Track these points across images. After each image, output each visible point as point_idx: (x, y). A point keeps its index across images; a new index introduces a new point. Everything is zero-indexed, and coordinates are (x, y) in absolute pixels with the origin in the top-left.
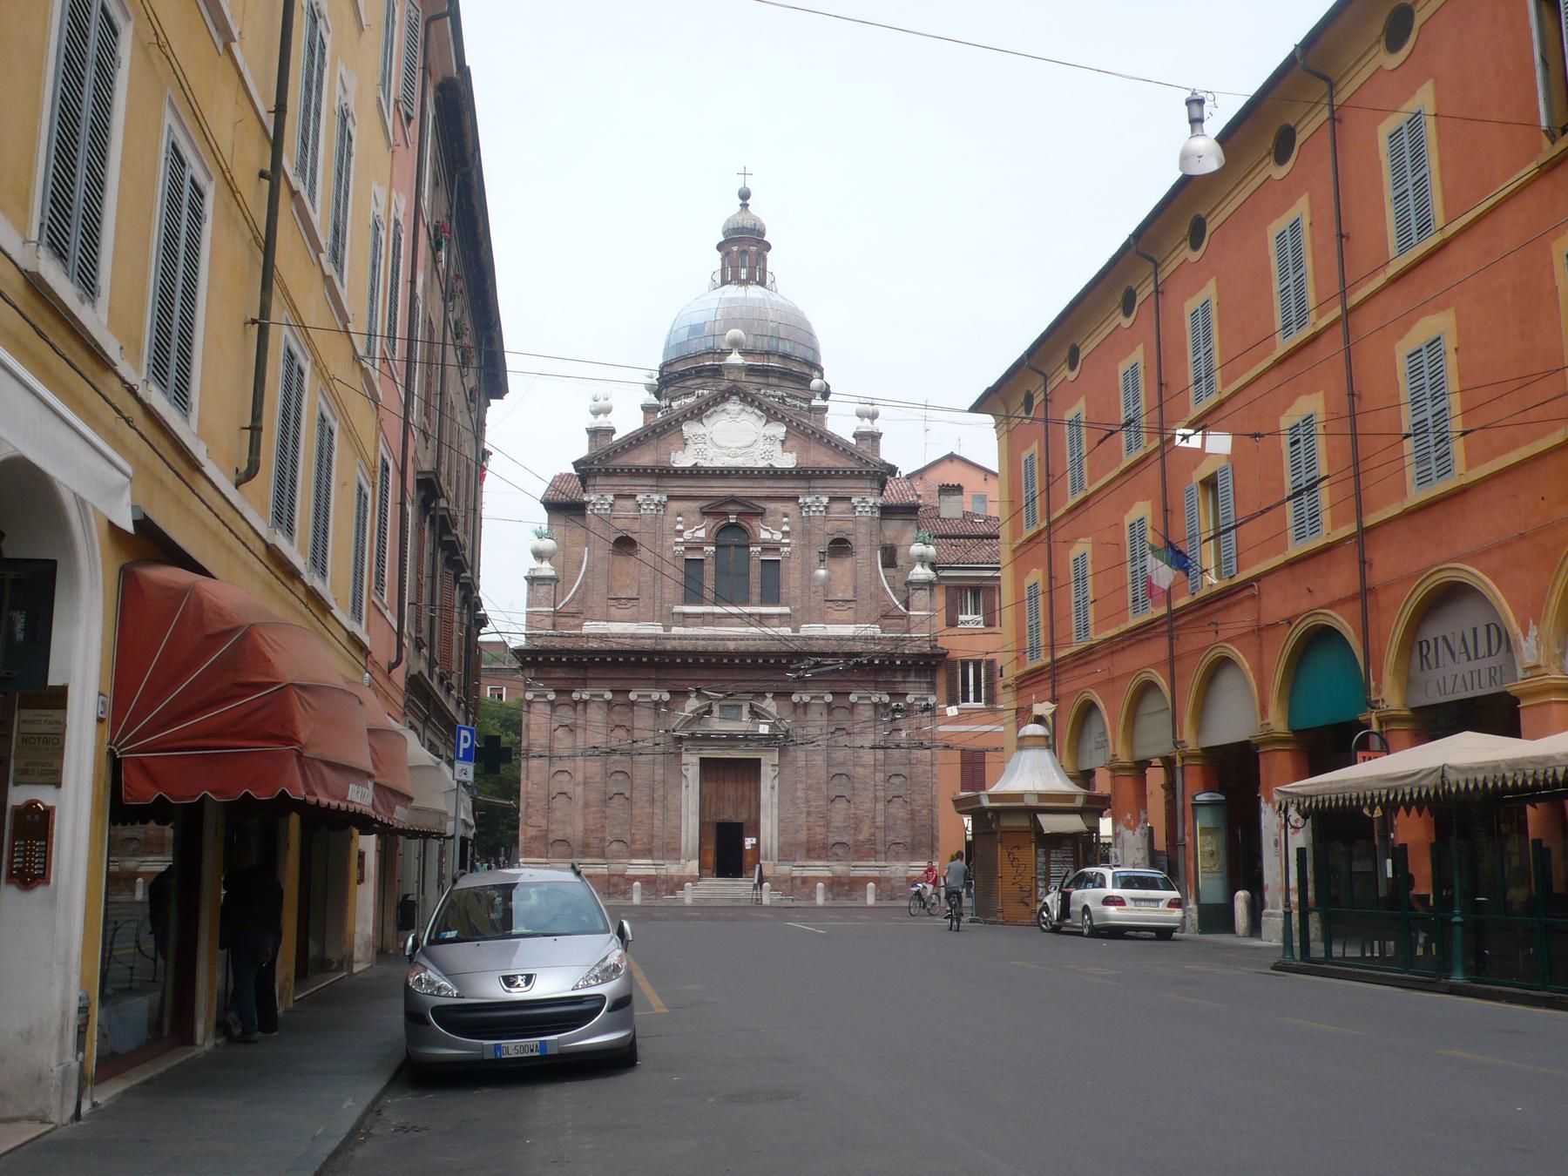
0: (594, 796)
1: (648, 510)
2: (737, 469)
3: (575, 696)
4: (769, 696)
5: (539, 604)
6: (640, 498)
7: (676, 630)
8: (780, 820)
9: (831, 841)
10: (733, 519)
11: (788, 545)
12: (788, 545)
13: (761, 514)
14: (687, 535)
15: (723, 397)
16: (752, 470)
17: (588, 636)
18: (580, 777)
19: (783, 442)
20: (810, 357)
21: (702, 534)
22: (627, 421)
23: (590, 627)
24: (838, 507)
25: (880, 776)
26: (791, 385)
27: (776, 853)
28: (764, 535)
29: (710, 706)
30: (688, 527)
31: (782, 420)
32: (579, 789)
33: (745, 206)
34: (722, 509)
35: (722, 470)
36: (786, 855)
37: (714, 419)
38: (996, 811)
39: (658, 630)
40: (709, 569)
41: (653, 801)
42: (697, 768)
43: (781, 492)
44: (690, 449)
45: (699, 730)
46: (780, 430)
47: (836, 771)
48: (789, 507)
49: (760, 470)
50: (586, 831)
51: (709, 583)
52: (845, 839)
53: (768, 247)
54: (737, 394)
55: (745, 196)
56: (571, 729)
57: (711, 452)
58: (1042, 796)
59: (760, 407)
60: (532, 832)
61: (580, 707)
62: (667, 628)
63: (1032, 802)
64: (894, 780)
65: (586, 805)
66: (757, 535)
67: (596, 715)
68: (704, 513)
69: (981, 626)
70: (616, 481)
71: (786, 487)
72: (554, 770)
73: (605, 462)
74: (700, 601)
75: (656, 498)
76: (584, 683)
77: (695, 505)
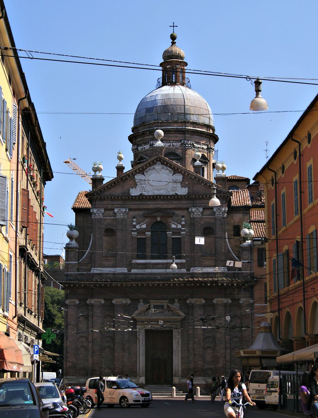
1: (120, 216)
2: (160, 196)
3: (88, 302)
4: (176, 300)
5: (71, 260)
6: (116, 210)
7: (133, 271)
8: (182, 358)
10: (159, 219)
13: (171, 215)
14: (138, 227)
15: (154, 163)
16: (167, 196)
17: (94, 274)
18: (90, 339)
19: (181, 183)
20: (207, 123)
21: (144, 226)
23: (95, 270)
24: (207, 212)
27: (180, 373)
28: (173, 226)
29: (150, 306)
30: (138, 223)
31: (180, 172)
32: (90, 345)
33: (173, 43)
34: (154, 215)
35: (153, 196)
37: (150, 172)
38: (248, 358)
39: (125, 270)
40: (149, 243)
42: (144, 334)
43: (180, 206)
44: (138, 187)
45: (143, 318)
46: (179, 177)
48: (184, 213)
49: (171, 196)
51: (148, 250)
52: (212, 366)
53: (186, 64)
54: (160, 161)
55: (173, 38)
56: (87, 317)
57: (148, 188)
58: (263, 352)
59: (170, 167)
60: (69, 364)
62: (129, 270)
63: (258, 354)
64: (234, 339)
65: (93, 352)
66: (170, 226)
67: (98, 312)
68: (145, 217)
69: (160, 321)
70: (105, 202)
71: (183, 204)
73: (99, 191)
74: (144, 258)
75: (124, 210)
76: (92, 297)
77: (142, 212)
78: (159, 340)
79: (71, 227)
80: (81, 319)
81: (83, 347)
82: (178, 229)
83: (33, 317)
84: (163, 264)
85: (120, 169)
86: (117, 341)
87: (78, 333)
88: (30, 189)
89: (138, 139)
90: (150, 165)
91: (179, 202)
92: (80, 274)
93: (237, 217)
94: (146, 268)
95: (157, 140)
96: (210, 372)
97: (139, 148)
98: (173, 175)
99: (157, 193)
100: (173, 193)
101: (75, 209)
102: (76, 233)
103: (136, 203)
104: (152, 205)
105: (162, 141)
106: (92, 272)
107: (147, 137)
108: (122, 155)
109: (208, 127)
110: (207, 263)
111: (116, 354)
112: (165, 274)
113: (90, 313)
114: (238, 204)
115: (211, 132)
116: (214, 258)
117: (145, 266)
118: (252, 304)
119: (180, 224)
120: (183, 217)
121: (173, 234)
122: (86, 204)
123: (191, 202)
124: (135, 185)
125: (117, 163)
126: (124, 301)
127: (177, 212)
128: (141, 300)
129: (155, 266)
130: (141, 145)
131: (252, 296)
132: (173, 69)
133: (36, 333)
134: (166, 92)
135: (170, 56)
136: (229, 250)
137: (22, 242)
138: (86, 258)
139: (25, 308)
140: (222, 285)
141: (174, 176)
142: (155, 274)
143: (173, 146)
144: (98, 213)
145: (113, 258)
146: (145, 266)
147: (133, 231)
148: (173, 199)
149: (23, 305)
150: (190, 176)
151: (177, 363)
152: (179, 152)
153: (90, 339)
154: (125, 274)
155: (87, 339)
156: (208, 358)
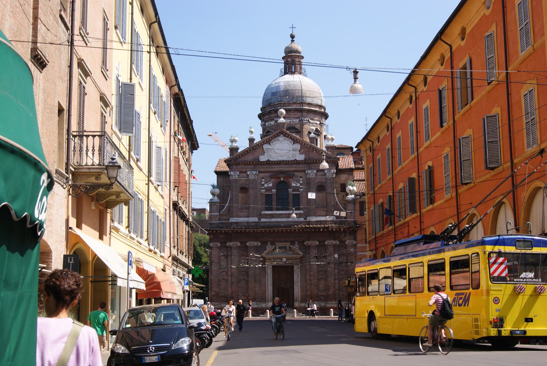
0: (234, 280)
1: (251, 177)
2: (283, 161)
3: (227, 245)
4: (296, 243)
5: (214, 212)
6: (248, 173)
7: (263, 220)
8: (301, 287)
9: (319, 294)
10: (282, 179)
11: (302, 188)
12: (302, 188)
13: (292, 176)
14: (266, 185)
15: (278, 135)
16: (288, 161)
17: (231, 223)
18: (229, 273)
19: (300, 151)
20: (319, 103)
21: (271, 185)
22: (243, 145)
23: (232, 220)
24: (320, 173)
25: (336, 271)
26: (312, 115)
27: (300, 299)
28: (294, 185)
30: (266, 183)
31: (299, 142)
32: (230, 278)
33: (292, 41)
34: (278, 176)
35: (277, 161)
36: (304, 299)
37: (275, 142)
39: (256, 219)
40: (274, 198)
41: (256, 281)
42: (271, 269)
43: (299, 169)
46: (298, 146)
47: (320, 269)
48: (302, 174)
49: (291, 161)
50: (232, 293)
51: (274, 203)
52: (324, 293)
53: (303, 57)
54: (283, 134)
55: (292, 37)
56: (226, 256)
60: (213, 293)
61: (229, 249)
62: (259, 219)
64: (342, 272)
65: (232, 283)
67: (235, 252)
68: (271, 177)
70: (240, 166)
71: (301, 167)
72: (221, 271)
73: (236, 159)
74: (271, 210)
76: (231, 241)
77: (269, 174)
78: (283, 274)
79: (213, 187)
80: (222, 258)
81: (223, 279)
82: (297, 187)
83: (184, 256)
84: (285, 214)
85: (251, 140)
86: (250, 274)
87: (220, 269)
88: (180, 156)
89: (266, 117)
90: (275, 137)
91: (297, 166)
92: (221, 223)
93: (343, 177)
94: (272, 218)
95: (280, 117)
96: (323, 298)
97: (267, 124)
99: (280, 159)
100: (293, 159)
101: (216, 172)
102: (217, 191)
103: (264, 167)
104: (276, 168)
105: (284, 118)
106: (230, 221)
107: (272, 115)
108: (253, 130)
109: (320, 106)
110: (320, 213)
111: (249, 285)
112: (287, 222)
113: (229, 253)
114: (344, 167)
115: (323, 111)
116: (325, 209)
117: (272, 216)
118: (356, 245)
119: (299, 183)
120: (301, 177)
121: (294, 191)
122: (225, 168)
123: (307, 165)
124: (263, 153)
125: (249, 136)
126: (256, 244)
127: (296, 174)
128: (269, 243)
129: (279, 216)
130: (268, 121)
131: (355, 239)
132: (292, 62)
133: (186, 269)
134: (287, 80)
136: (337, 203)
137: (175, 198)
138: (225, 210)
139: (178, 249)
140: (332, 230)
142: (280, 222)
143: (293, 122)
144: (235, 175)
145: (247, 210)
146: (272, 216)
147: (262, 189)
148: (293, 164)
149: (176, 248)
151: (297, 291)
152: (298, 126)
153: (229, 273)
154: (256, 222)
155: (227, 273)
156: (322, 287)
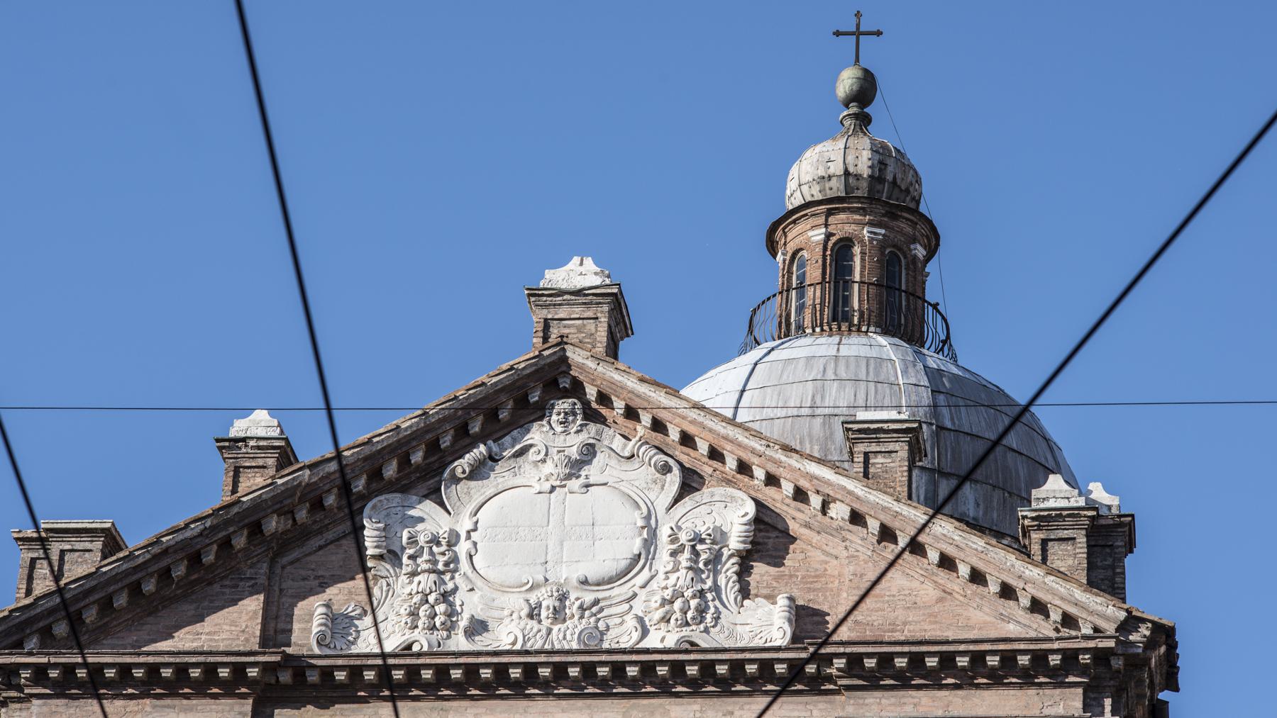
98: (676, 500)
135: (830, 177)
141: (687, 502)
150: (816, 501)
